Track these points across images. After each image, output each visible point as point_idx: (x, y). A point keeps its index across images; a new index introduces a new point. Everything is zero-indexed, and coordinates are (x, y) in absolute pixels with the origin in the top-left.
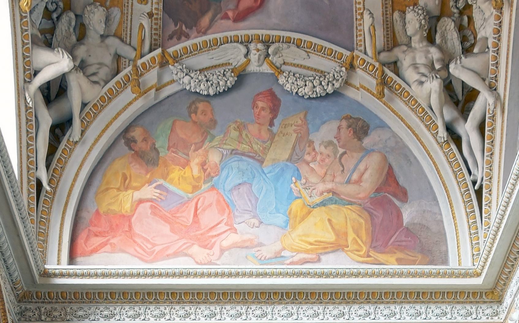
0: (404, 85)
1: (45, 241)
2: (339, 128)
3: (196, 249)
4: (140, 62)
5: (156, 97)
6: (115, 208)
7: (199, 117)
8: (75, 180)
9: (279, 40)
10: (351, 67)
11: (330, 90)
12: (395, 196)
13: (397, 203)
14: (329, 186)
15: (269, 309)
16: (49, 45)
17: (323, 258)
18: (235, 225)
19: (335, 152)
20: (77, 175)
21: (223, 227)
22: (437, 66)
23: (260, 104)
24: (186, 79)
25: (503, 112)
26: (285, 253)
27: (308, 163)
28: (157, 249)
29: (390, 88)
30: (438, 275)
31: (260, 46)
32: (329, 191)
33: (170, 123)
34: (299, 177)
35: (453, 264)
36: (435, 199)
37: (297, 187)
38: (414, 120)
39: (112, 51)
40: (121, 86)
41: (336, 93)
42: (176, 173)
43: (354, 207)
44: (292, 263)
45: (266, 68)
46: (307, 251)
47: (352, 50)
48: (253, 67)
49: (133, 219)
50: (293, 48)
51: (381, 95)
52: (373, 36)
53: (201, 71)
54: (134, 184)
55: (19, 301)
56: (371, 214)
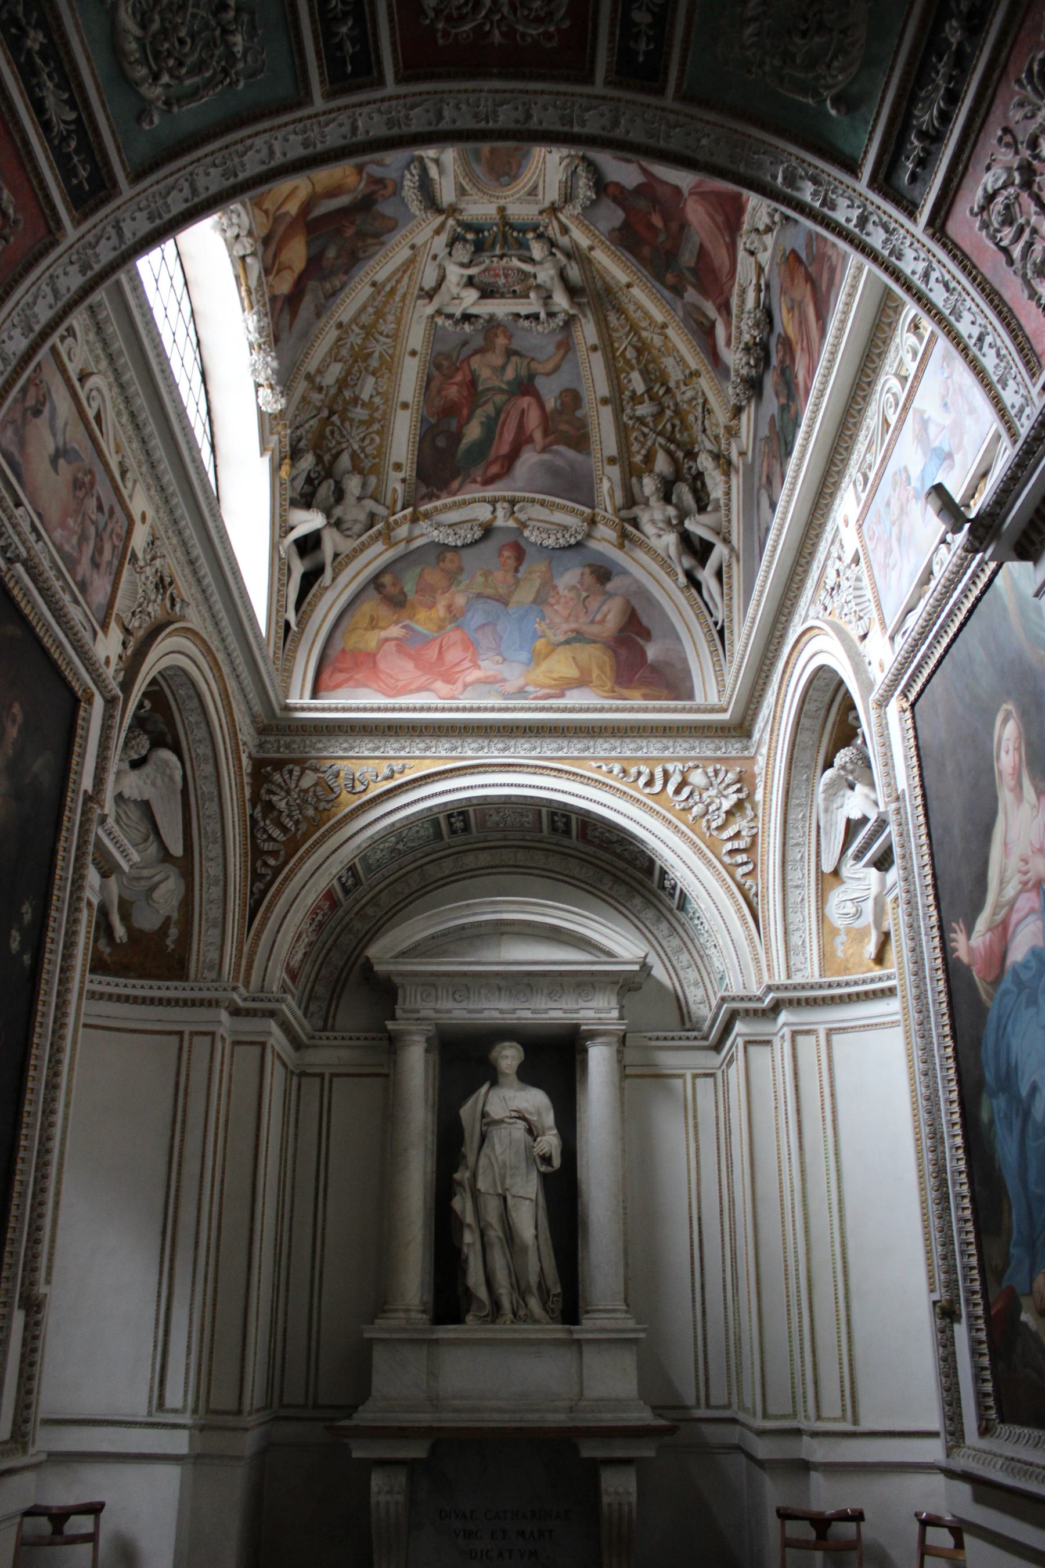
0: (643, 538)
1: (290, 677)
2: (582, 574)
3: (439, 685)
4: (392, 519)
5: (406, 547)
6: (361, 646)
7: (448, 565)
8: (323, 621)
9: (523, 500)
10: (592, 522)
11: (573, 541)
12: (638, 634)
13: (641, 642)
14: (573, 626)
15: (512, 742)
16: (308, 506)
17: (568, 693)
18: (480, 663)
19: (579, 596)
20: (326, 616)
21: (466, 664)
22: (674, 522)
23: (506, 554)
24: (436, 533)
25: (738, 561)
26: (530, 689)
27: (552, 605)
28: (400, 684)
29: (631, 540)
30: (683, 710)
31: (506, 505)
32: (573, 631)
33: (418, 570)
34: (543, 618)
35: (699, 700)
36: (678, 638)
37: (540, 627)
38: (655, 567)
39: (367, 510)
40: (374, 539)
41: (579, 544)
42: (422, 614)
43: (598, 645)
44: (535, 698)
45: (511, 523)
46: (551, 687)
47: (593, 508)
48: (500, 522)
49: (378, 657)
50: (537, 507)
51: (621, 546)
52: (612, 496)
53: (450, 526)
54: (381, 624)
55: (259, 734)
56: (616, 654)
